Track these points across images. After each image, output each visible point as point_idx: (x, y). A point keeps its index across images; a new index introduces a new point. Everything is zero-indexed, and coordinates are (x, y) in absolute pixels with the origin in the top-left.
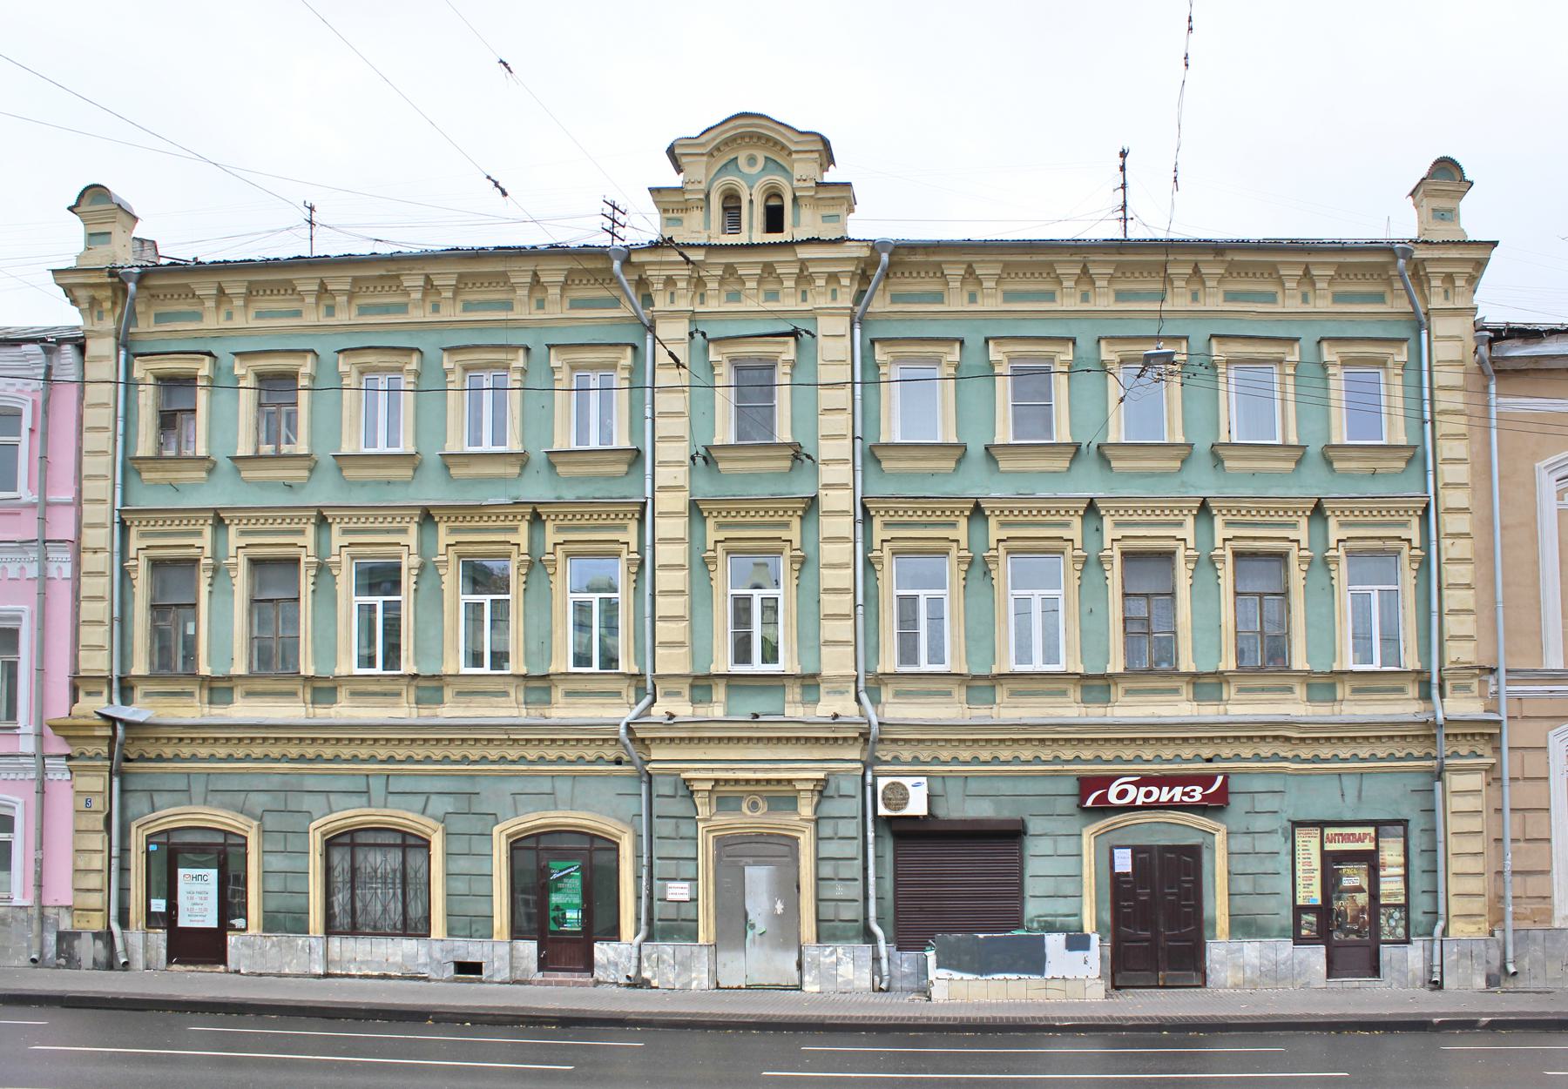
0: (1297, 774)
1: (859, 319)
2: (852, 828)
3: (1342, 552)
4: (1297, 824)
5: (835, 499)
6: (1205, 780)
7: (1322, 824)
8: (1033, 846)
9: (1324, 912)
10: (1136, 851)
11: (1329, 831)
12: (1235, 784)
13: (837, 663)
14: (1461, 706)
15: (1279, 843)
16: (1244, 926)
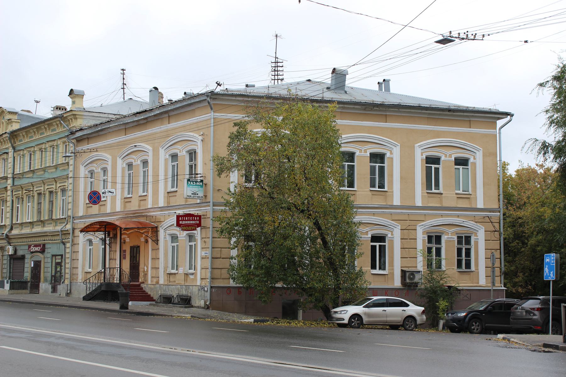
0: (52, 243)
1: (14, 148)
2: (5, 257)
3: (59, 190)
4: (53, 256)
5: (9, 188)
6: (39, 245)
7: (56, 256)
8: (26, 261)
9: (55, 276)
10: (34, 262)
11: (57, 257)
12: (47, 246)
13: (8, 222)
14: (69, 227)
15: (50, 260)
16: (46, 280)
